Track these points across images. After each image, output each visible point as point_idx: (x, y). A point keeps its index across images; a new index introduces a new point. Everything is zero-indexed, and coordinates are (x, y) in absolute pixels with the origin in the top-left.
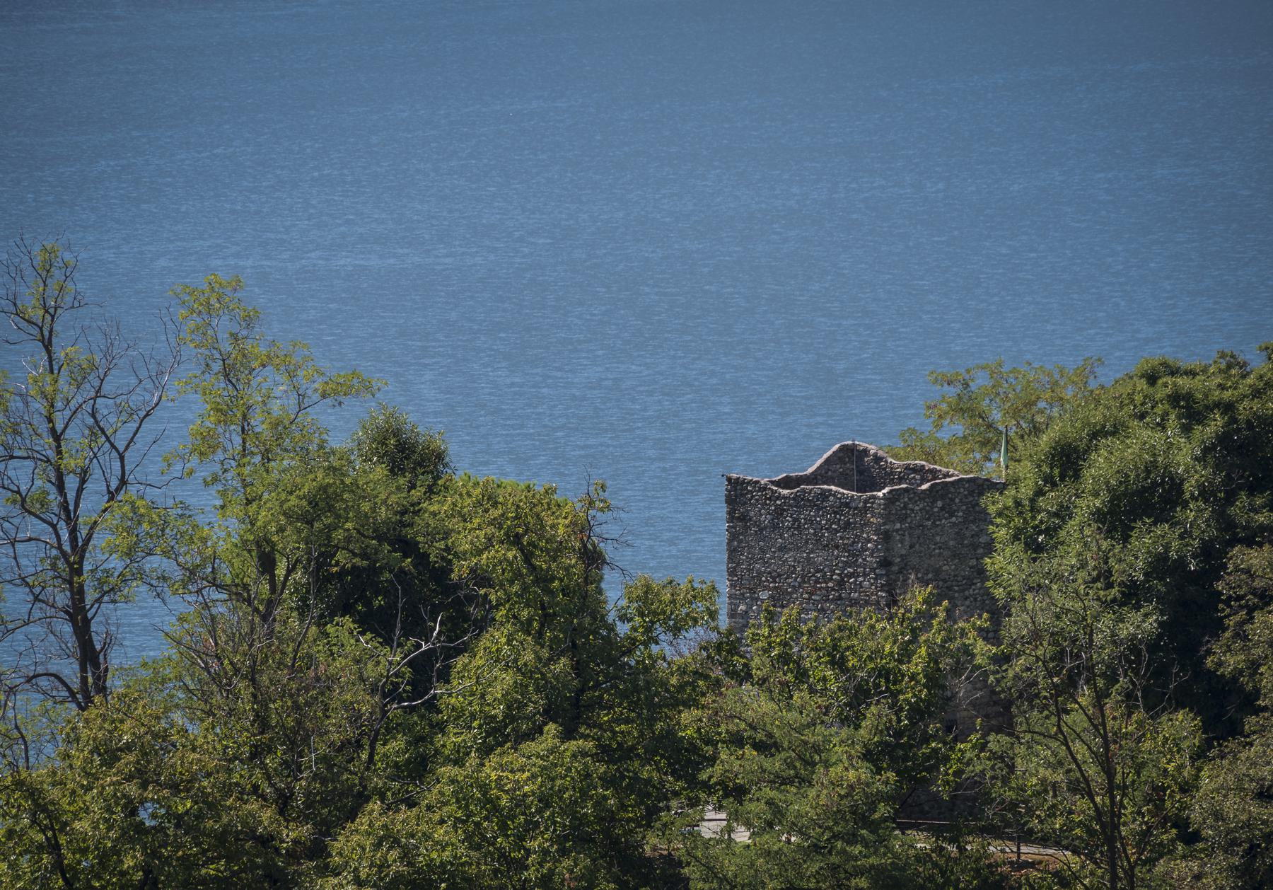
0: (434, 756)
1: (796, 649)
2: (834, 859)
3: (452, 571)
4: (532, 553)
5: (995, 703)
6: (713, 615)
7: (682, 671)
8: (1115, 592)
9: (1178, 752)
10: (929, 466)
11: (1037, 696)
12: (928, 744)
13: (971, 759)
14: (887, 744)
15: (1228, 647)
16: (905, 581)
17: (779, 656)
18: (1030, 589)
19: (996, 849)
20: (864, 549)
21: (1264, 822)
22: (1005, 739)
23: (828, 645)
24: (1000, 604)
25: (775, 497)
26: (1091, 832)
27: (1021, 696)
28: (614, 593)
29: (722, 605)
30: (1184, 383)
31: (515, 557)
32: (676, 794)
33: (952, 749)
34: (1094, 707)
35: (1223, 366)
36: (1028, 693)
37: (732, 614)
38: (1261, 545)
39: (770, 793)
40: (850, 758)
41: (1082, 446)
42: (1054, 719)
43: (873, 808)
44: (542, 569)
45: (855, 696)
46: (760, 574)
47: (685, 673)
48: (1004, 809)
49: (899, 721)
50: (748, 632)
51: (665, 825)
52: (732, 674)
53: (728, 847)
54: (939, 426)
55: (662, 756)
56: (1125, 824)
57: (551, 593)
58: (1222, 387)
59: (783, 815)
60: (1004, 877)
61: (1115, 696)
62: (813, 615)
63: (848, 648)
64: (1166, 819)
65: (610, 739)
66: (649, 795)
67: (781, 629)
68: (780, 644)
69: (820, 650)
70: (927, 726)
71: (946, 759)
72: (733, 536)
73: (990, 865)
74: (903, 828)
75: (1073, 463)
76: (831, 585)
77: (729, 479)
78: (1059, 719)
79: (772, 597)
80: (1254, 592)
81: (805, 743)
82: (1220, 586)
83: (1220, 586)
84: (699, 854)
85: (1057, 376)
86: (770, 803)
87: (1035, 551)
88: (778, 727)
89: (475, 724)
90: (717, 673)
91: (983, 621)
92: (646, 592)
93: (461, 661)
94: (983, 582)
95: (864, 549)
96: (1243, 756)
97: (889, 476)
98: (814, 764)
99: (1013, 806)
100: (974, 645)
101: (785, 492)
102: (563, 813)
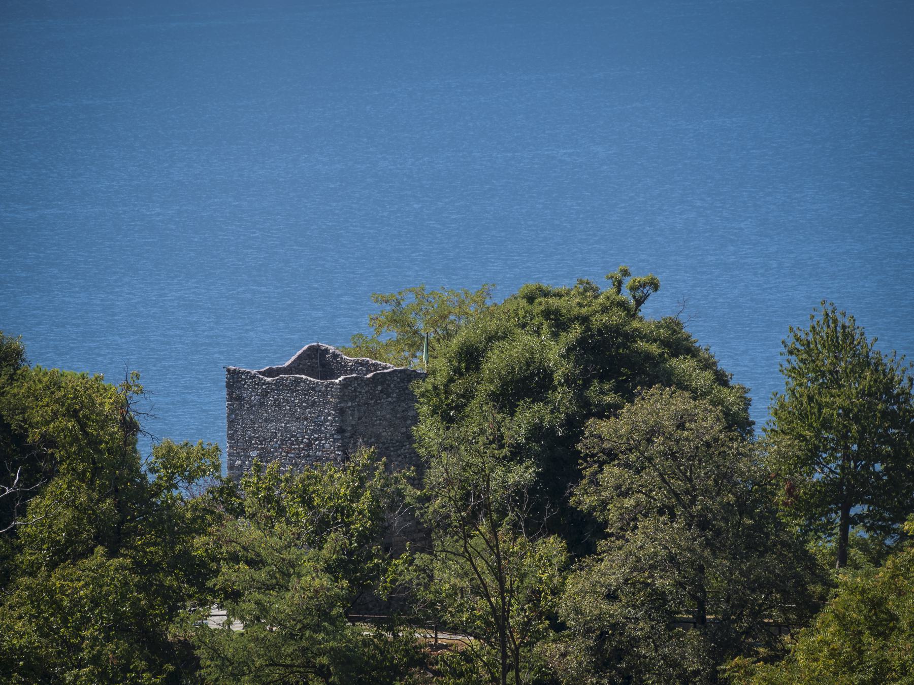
0: (15, 569)
1: (276, 493)
2: (304, 643)
3: (28, 436)
4: (86, 423)
5: (420, 531)
6: (217, 468)
7: (195, 508)
8: (506, 451)
9: (550, 566)
10: (372, 361)
11: (450, 525)
12: (372, 560)
13: (403, 571)
14: (342, 560)
15: (585, 490)
16: (355, 443)
17: (265, 497)
18: (445, 449)
19: (421, 635)
20: (326, 420)
21: (611, 616)
22: (426, 556)
23: (299, 489)
24: (423, 460)
25: (261, 383)
26: (488, 623)
27: (438, 525)
28: (146, 452)
29: (224, 460)
30: (554, 302)
31: (74, 426)
32: (190, 596)
33: (389, 564)
34: (490, 533)
35: (581, 290)
36: (444, 524)
37: (231, 467)
38: (608, 417)
39: (259, 596)
40: (316, 570)
41: (481, 346)
42: (462, 542)
43: (332, 606)
44: (93, 435)
45: (319, 526)
46: (251, 438)
47: (196, 509)
48: (426, 607)
49: (351, 544)
50: (242, 481)
51: (182, 620)
52: (231, 511)
53: (228, 635)
54: (379, 333)
55: (180, 570)
56: (512, 617)
57: (100, 452)
58: (580, 305)
59: (267, 612)
60: (426, 656)
61: (506, 527)
62: (289, 467)
63: (314, 492)
64: (542, 613)
65: (142, 557)
66: (170, 598)
67: (266, 478)
68: (265, 489)
69: (294, 493)
70: (371, 547)
71: (385, 571)
72: (231, 411)
73: (416, 647)
74: (353, 620)
75: (475, 359)
76: (302, 446)
77: (229, 370)
78: (466, 542)
79: (259, 455)
80: (603, 451)
81: (283, 560)
82: (579, 447)
83: (579, 447)
84: (207, 640)
85: (463, 297)
86: (258, 603)
87: (449, 422)
88: (264, 548)
89: (45, 547)
90: (220, 509)
91: (411, 472)
92: (169, 452)
93: (34, 501)
94: (411, 444)
95: (326, 420)
96: (596, 568)
97: (343, 368)
98: (289, 575)
99: (432, 604)
100: (405, 489)
101: (269, 379)
102: (109, 610)
